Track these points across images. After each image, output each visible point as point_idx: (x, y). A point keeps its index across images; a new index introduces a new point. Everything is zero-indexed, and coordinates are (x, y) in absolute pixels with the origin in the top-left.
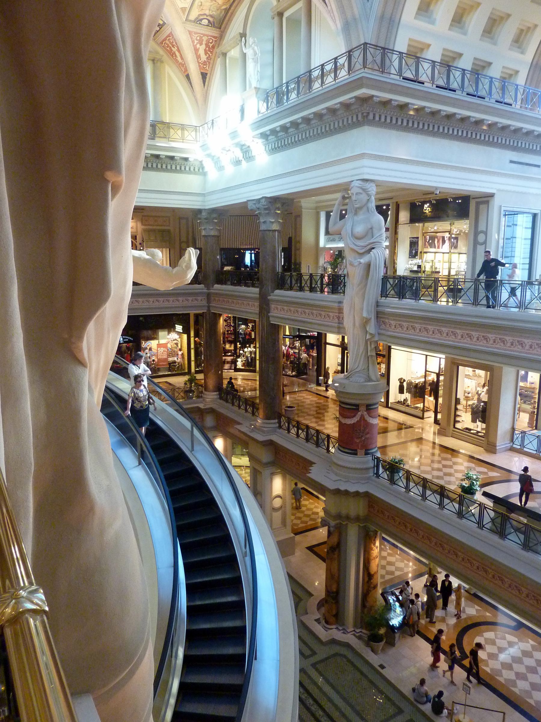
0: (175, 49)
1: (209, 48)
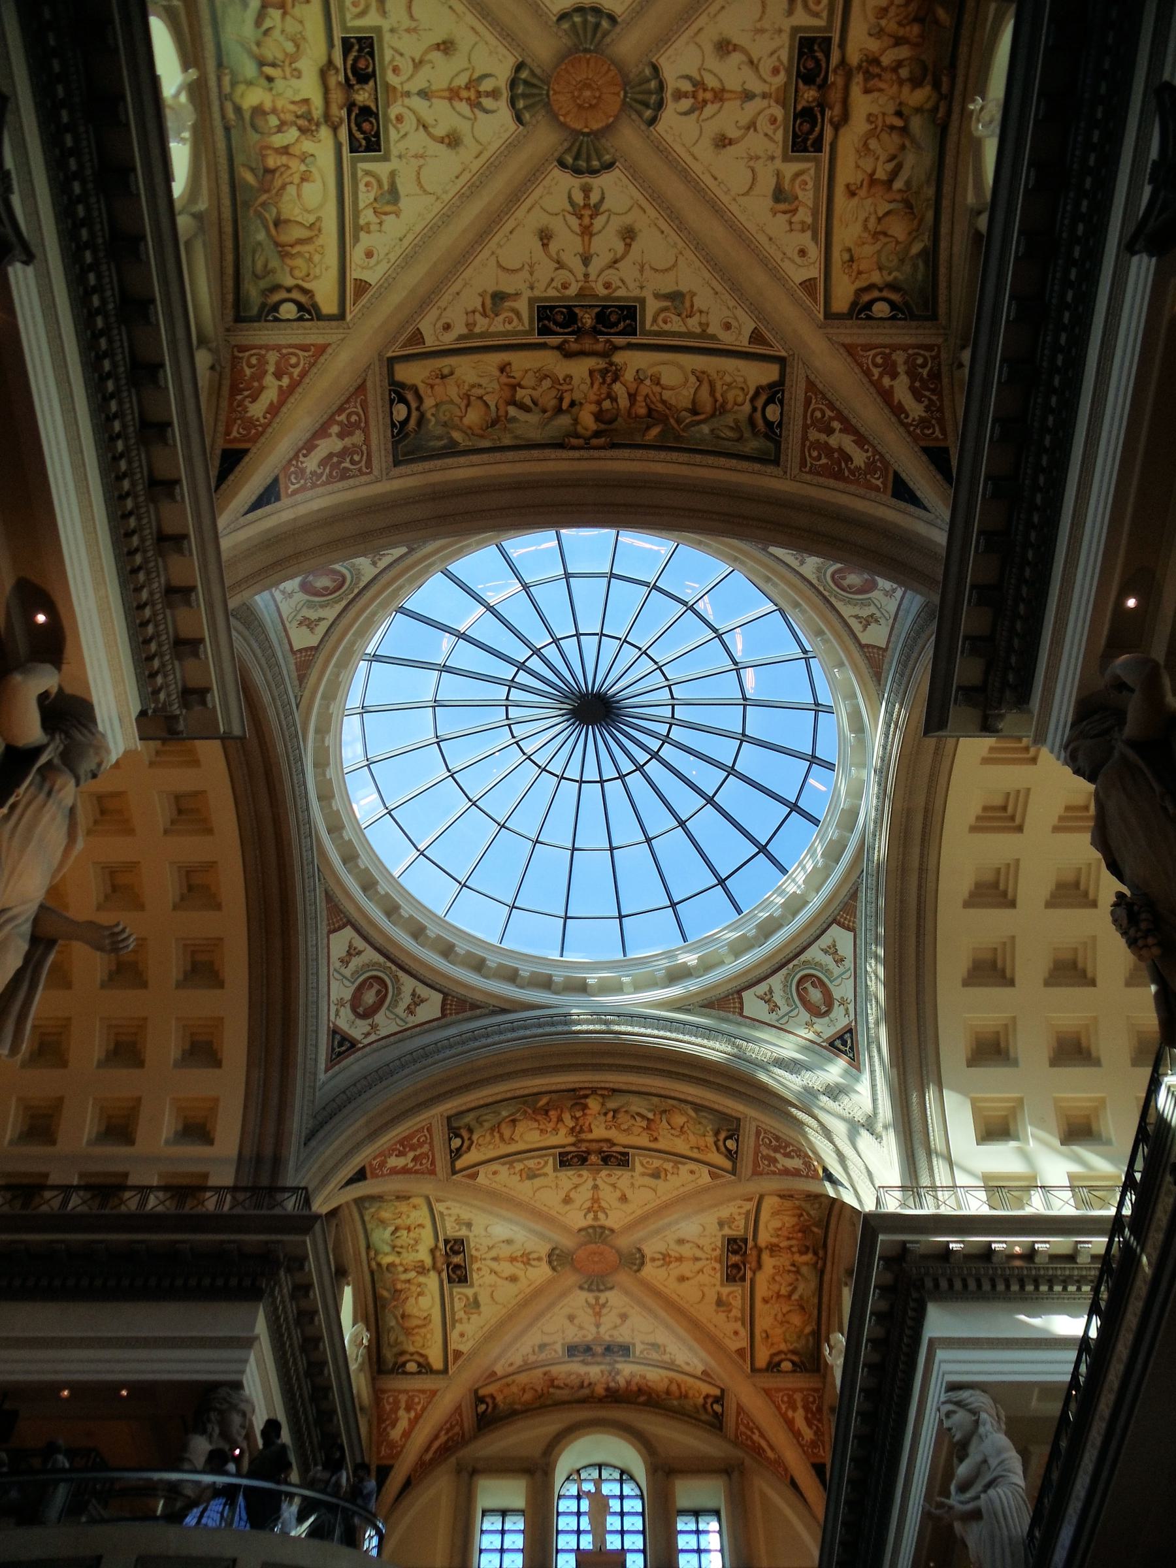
0: (756, 1437)
1: (812, 1412)
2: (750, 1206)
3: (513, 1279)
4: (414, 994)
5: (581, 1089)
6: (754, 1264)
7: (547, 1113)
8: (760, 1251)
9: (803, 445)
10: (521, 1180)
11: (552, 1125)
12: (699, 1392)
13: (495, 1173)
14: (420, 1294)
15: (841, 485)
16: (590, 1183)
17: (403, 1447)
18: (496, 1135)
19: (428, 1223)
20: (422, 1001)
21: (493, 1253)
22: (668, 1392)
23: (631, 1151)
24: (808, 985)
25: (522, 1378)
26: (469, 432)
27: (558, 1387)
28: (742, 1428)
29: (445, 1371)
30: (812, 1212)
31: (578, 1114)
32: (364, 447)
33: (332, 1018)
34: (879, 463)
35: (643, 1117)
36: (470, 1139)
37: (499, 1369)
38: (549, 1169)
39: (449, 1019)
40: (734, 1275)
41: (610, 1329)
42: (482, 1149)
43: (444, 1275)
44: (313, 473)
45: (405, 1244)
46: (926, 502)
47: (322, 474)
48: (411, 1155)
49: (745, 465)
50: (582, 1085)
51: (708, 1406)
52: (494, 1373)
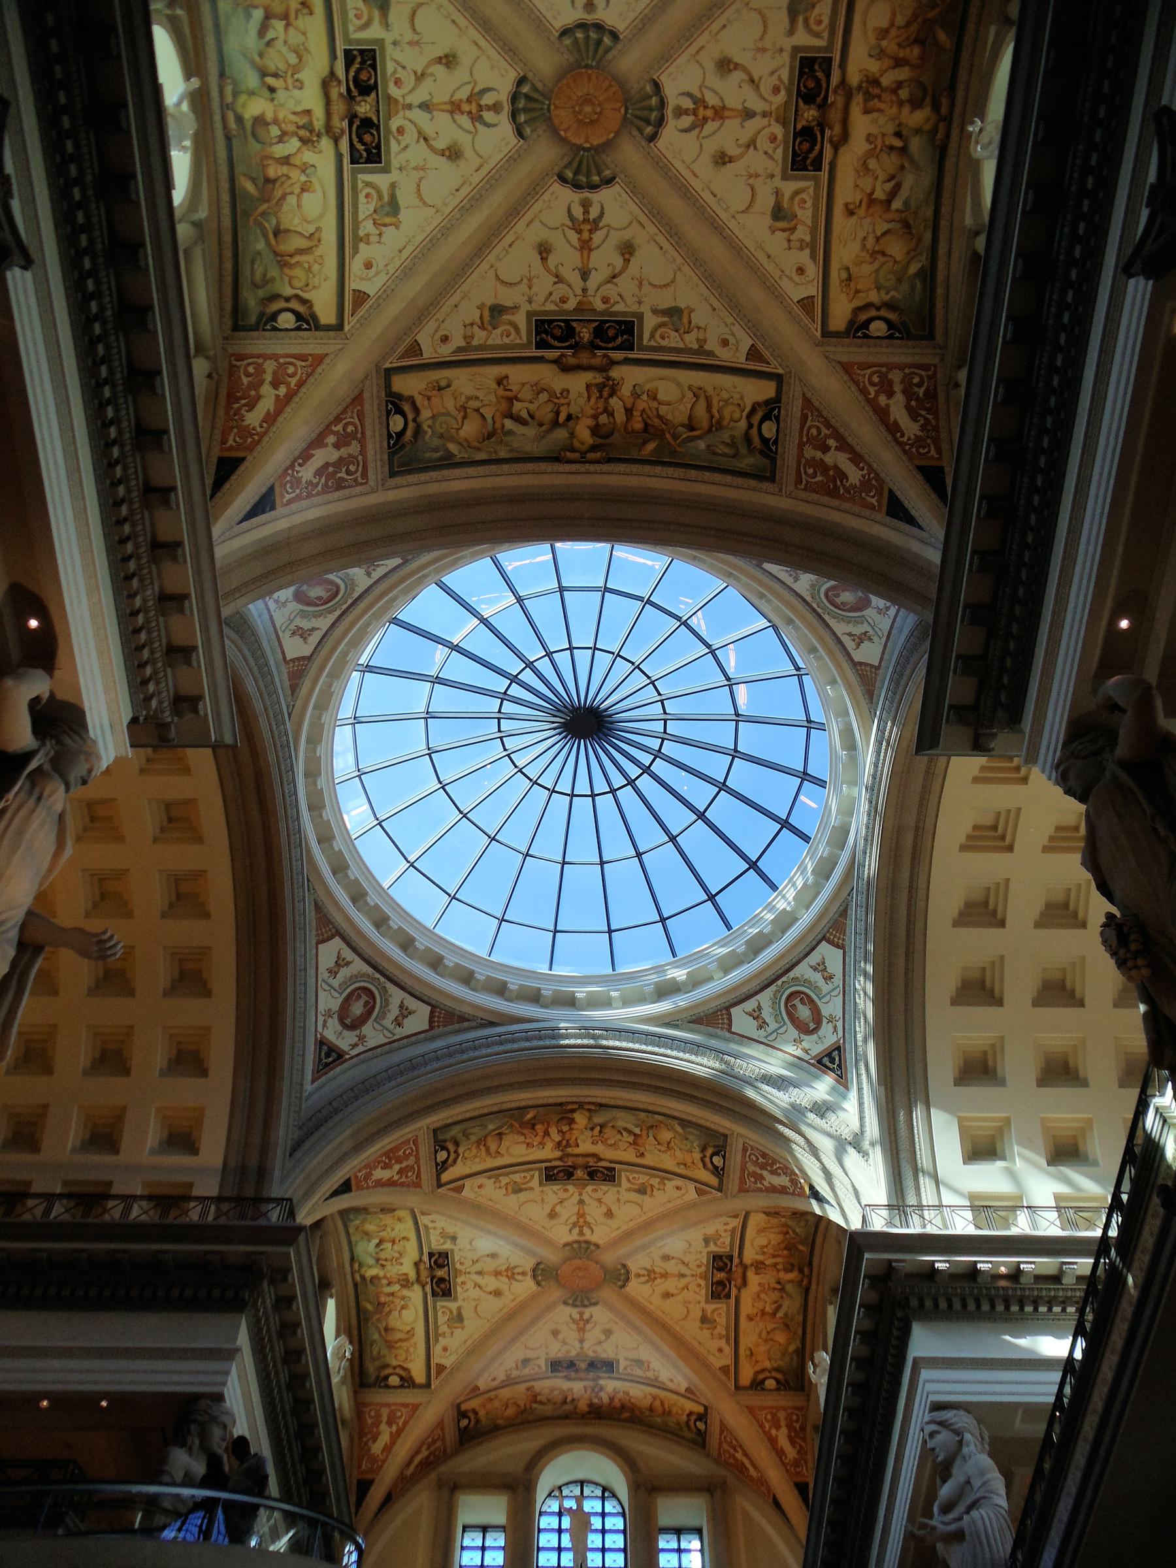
0: (739, 1455)
1: (796, 1431)
2: (736, 1223)
3: (497, 1293)
4: (401, 1006)
5: (568, 1103)
6: (739, 1281)
7: (533, 1127)
8: (745, 1268)
9: (799, 462)
10: (507, 1194)
11: (538, 1139)
12: (683, 1409)
13: (480, 1187)
14: (403, 1308)
15: (836, 503)
16: (576, 1198)
17: (384, 1461)
18: (482, 1147)
19: (412, 1235)
20: (410, 1013)
21: (478, 1267)
22: (651, 1409)
23: (617, 1166)
24: (797, 1002)
25: (505, 1393)
26: (465, 444)
27: (541, 1403)
28: (725, 1446)
29: (428, 1385)
30: (798, 1230)
31: (565, 1128)
32: (360, 458)
33: (320, 1029)
34: (874, 481)
35: (630, 1132)
36: (456, 1152)
37: (482, 1384)
38: (535, 1182)
39: (437, 1031)
40: (719, 1291)
41: (594, 1345)
42: (468, 1162)
43: (428, 1289)
44: (309, 483)
45: (389, 1257)
46: (920, 521)
47: (318, 484)
48: (397, 1167)
49: (739, 481)
50: (569, 1100)
51: (692, 1424)
52: (477, 1388)
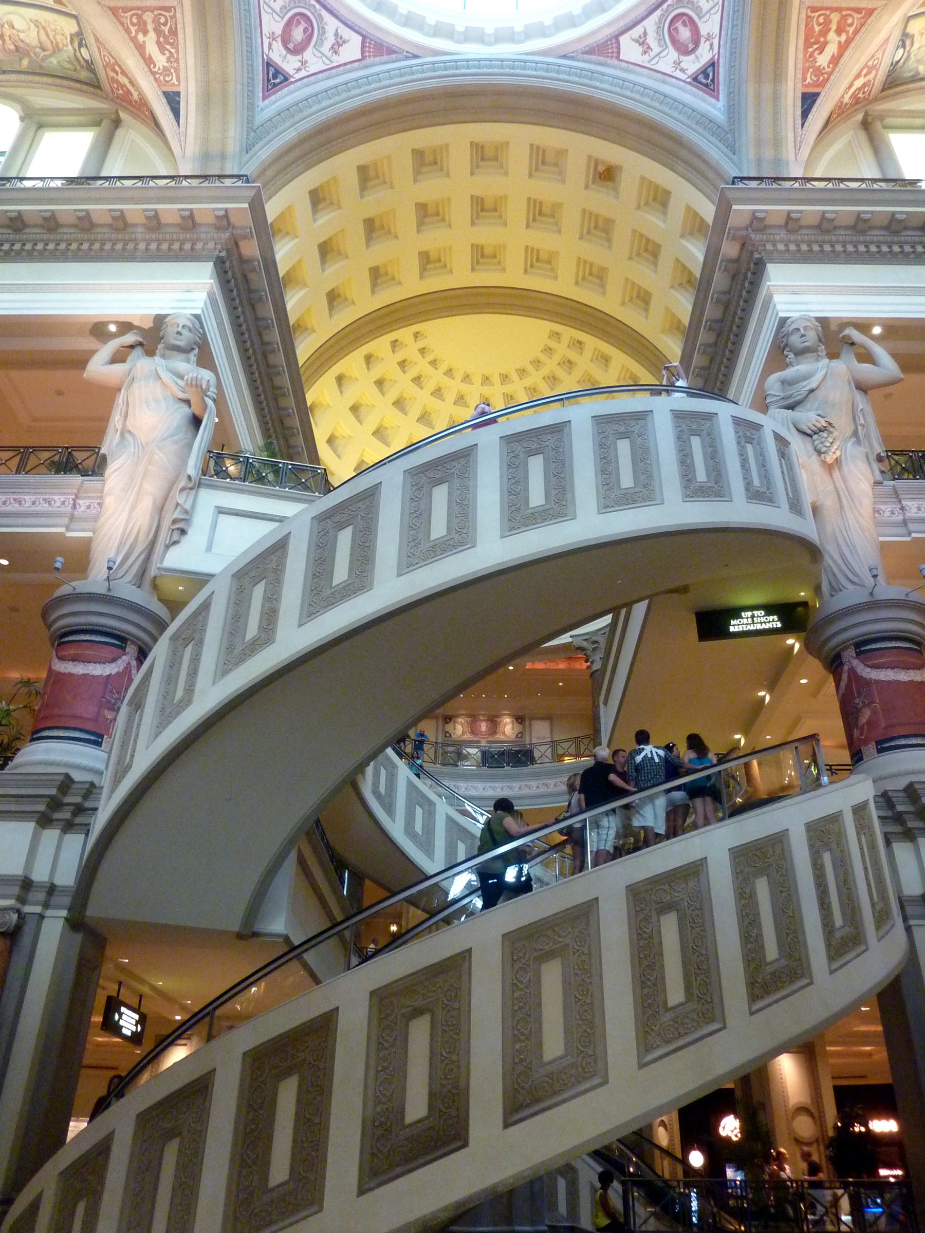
4: (336, 34)
20: (344, 42)
24: (679, 25)
39: (368, 61)
